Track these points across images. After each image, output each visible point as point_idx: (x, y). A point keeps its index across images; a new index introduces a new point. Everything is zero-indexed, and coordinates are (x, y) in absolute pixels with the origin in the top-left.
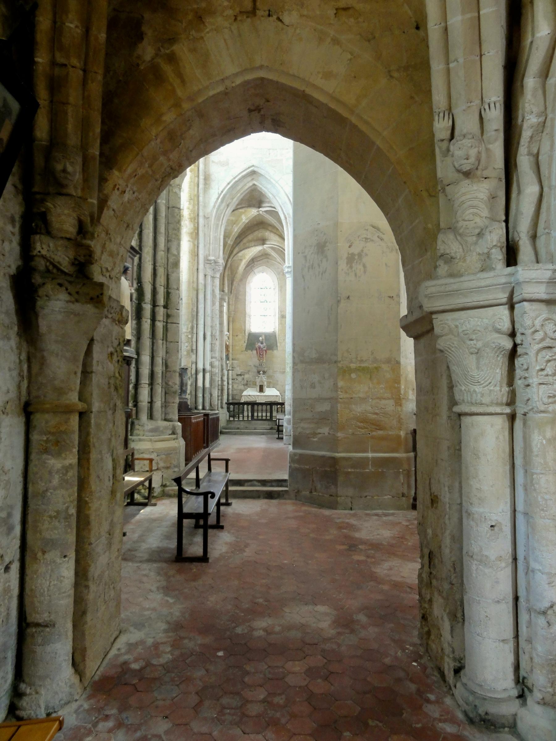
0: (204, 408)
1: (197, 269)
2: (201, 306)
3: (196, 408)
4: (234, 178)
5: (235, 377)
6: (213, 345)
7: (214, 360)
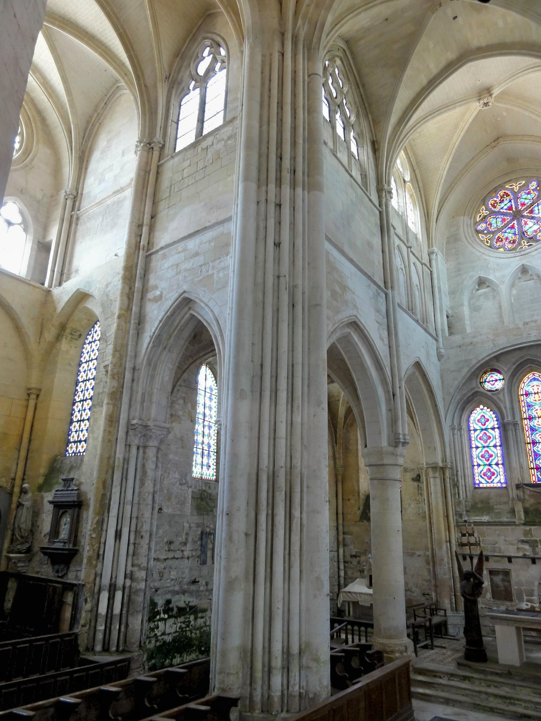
0: (106, 649)
1: (117, 439)
2: (116, 491)
3: (90, 649)
4: (167, 313)
5: (348, 558)
6: (136, 545)
7: (135, 569)
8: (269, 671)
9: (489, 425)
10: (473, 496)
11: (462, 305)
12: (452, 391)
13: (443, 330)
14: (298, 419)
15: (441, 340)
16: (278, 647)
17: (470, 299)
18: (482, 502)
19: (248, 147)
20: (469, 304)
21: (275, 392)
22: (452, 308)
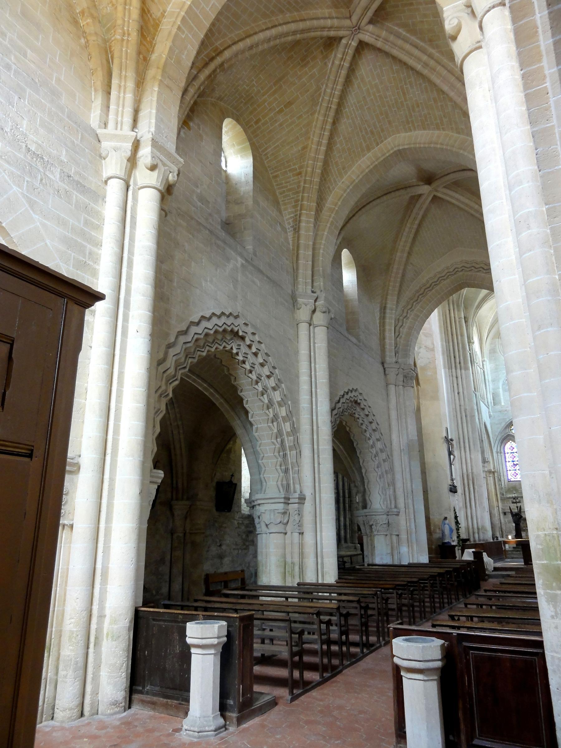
8: (474, 533)
9: (515, 450)
10: (508, 485)
11: (499, 388)
12: (497, 434)
13: (491, 403)
14: (473, 457)
15: (490, 408)
16: (475, 526)
17: (503, 385)
18: (513, 488)
19: (443, 354)
20: (502, 388)
21: (465, 448)
22: (493, 389)
